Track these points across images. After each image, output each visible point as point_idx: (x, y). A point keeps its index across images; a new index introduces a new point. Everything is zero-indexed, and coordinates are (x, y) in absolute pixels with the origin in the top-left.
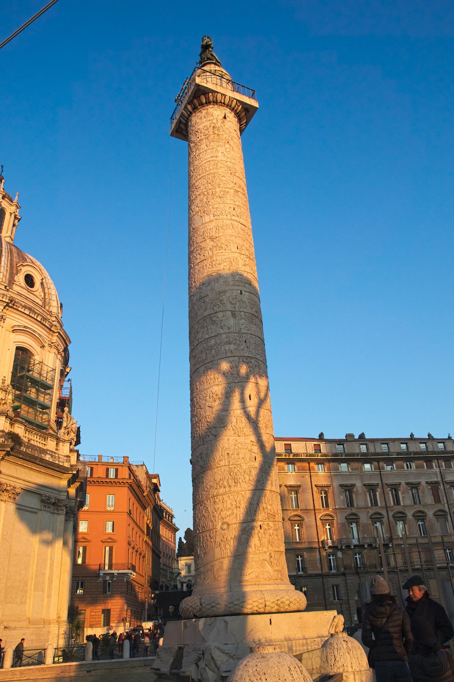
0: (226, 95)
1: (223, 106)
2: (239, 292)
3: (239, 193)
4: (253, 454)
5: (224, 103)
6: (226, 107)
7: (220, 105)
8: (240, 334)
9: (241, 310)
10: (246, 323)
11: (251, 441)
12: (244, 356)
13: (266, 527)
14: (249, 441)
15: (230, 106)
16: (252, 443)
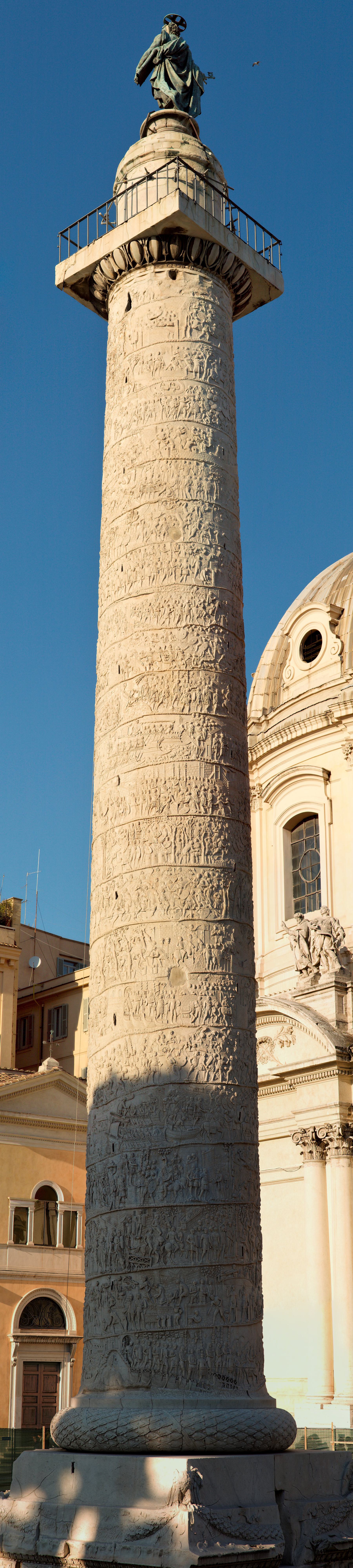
0: (112, 253)
1: (125, 275)
2: (116, 780)
3: (138, 510)
4: (111, 1139)
5: (120, 271)
6: (130, 272)
7: (119, 280)
8: (110, 882)
9: (115, 824)
10: (122, 851)
11: (112, 1114)
12: (111, 931)
13: (124, 1285)
14: (108, 1114)
15: (134, 263)
16: (113, 1116)
